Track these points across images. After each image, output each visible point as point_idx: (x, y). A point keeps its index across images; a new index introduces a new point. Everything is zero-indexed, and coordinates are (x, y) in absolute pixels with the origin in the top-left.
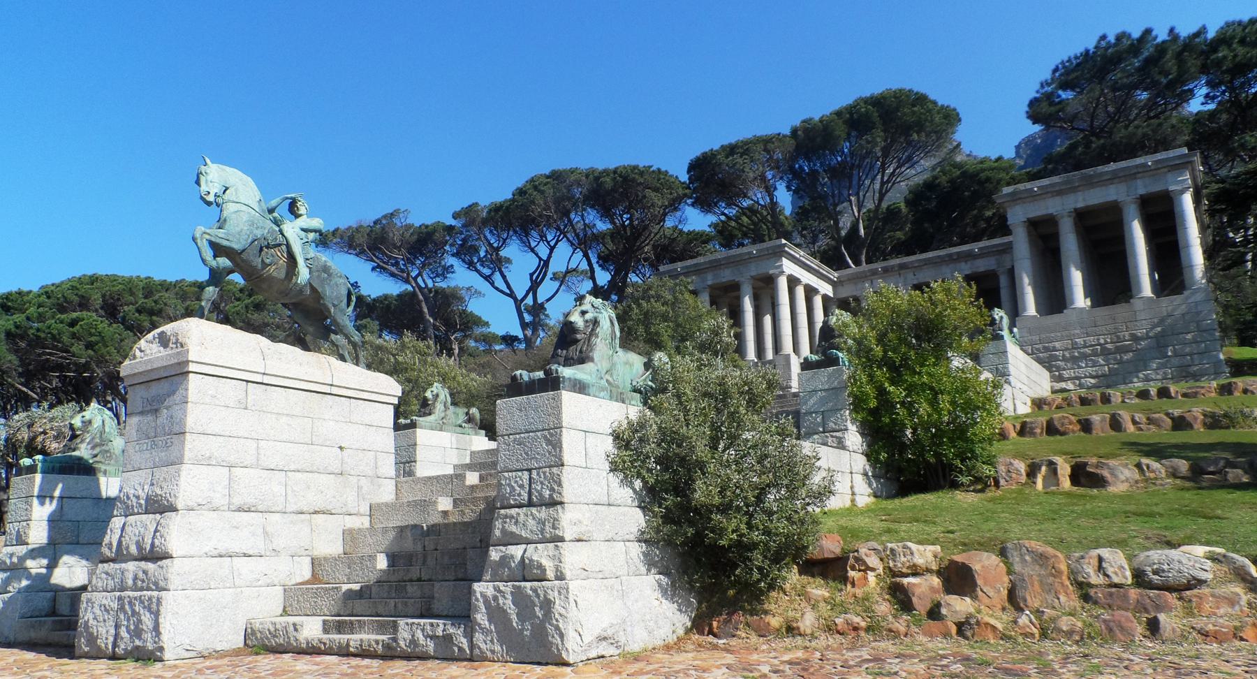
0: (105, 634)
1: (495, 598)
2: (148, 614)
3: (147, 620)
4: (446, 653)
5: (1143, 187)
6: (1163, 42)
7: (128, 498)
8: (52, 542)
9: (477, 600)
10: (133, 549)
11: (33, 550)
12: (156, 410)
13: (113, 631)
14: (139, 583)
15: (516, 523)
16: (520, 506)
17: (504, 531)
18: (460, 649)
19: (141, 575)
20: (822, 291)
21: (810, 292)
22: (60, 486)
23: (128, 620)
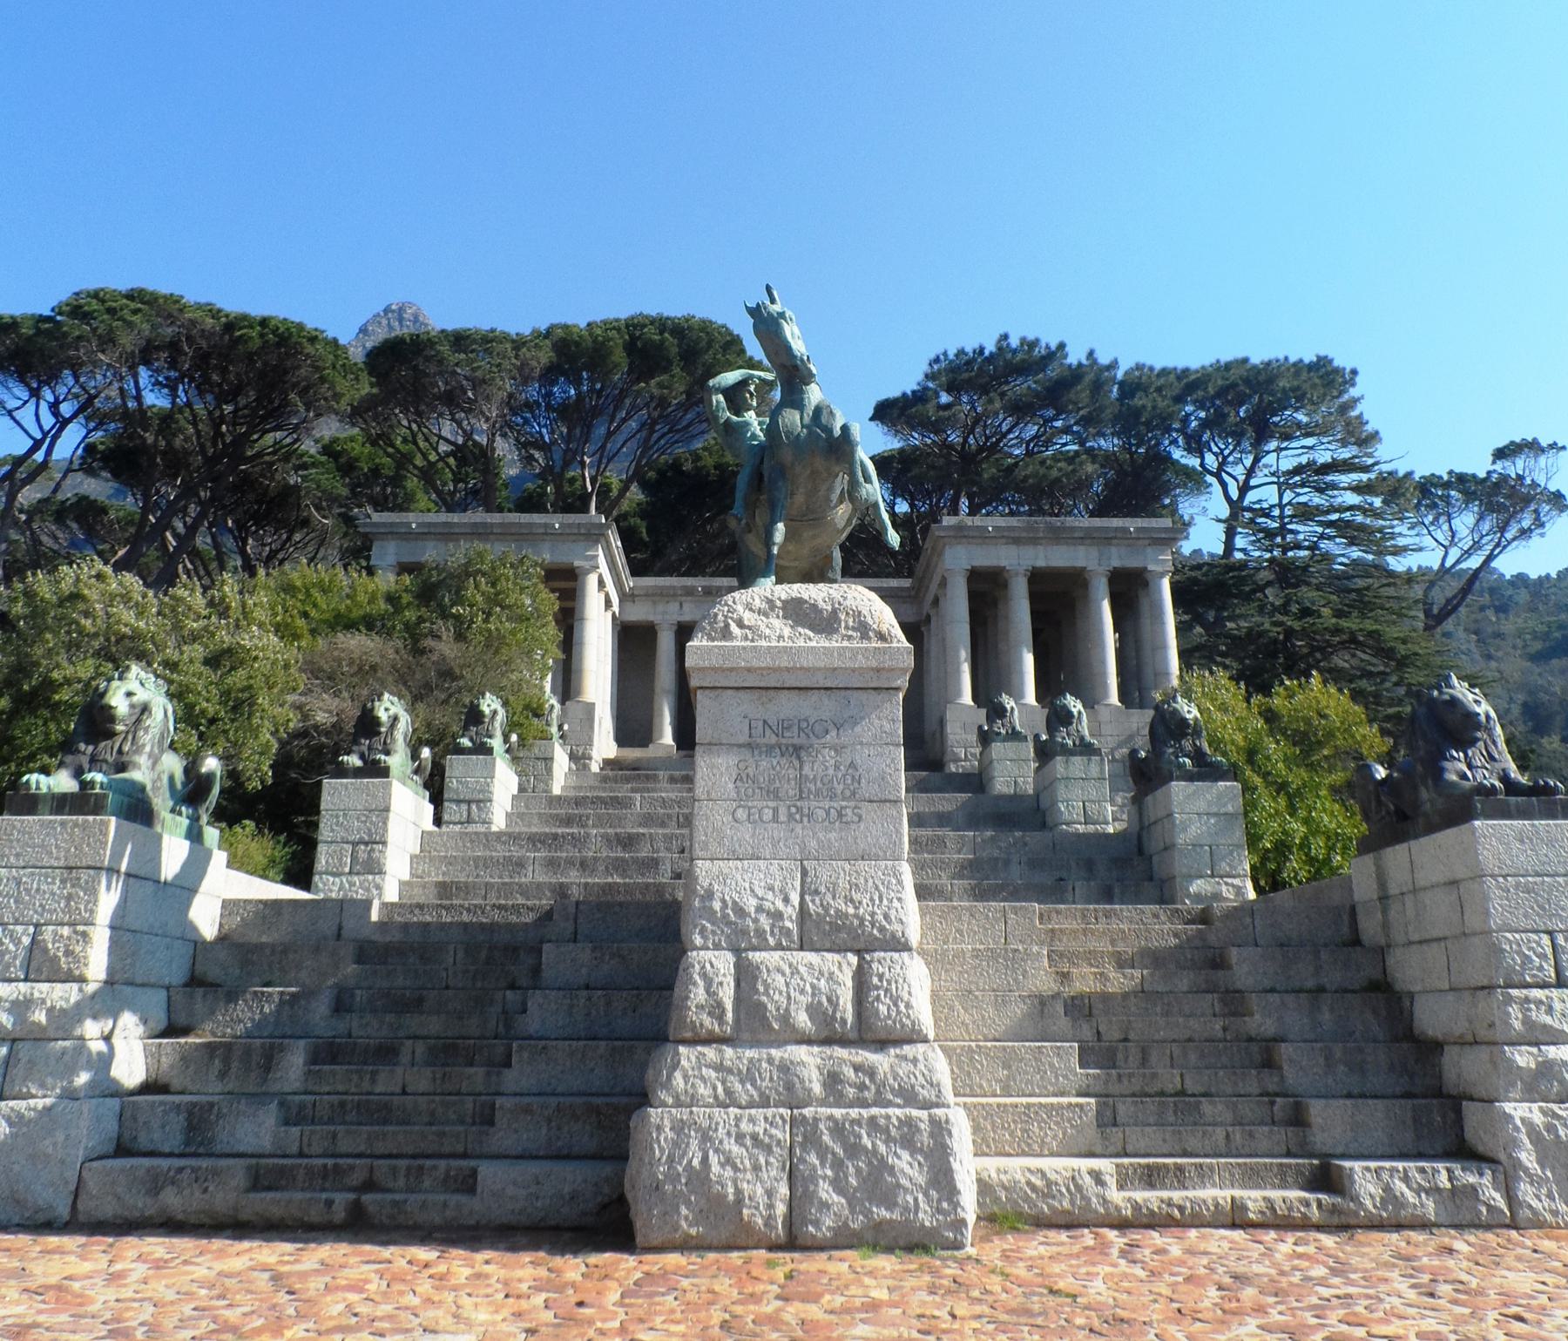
0: (764, 1195)
1: (1550, 1128)
2: (905, 1155)
3: (908, 1168)
4: (1462, 1213)
5: (1119, 558)
6: (1080, 365)
7: (740, 911)
8: (109, 983)
9: (1517, 1129)
10: (802, 1020)
11: (94, 996)
12: (797, 750)
13: (784, 1190)
14: (851, 1092)
15: (1550, 1011)
16: (1544, 985)
17: (1527, 1021)
18: (1490, 1208)
19: (849, 1073)
22: (129, 847)
23: (838, 1165)
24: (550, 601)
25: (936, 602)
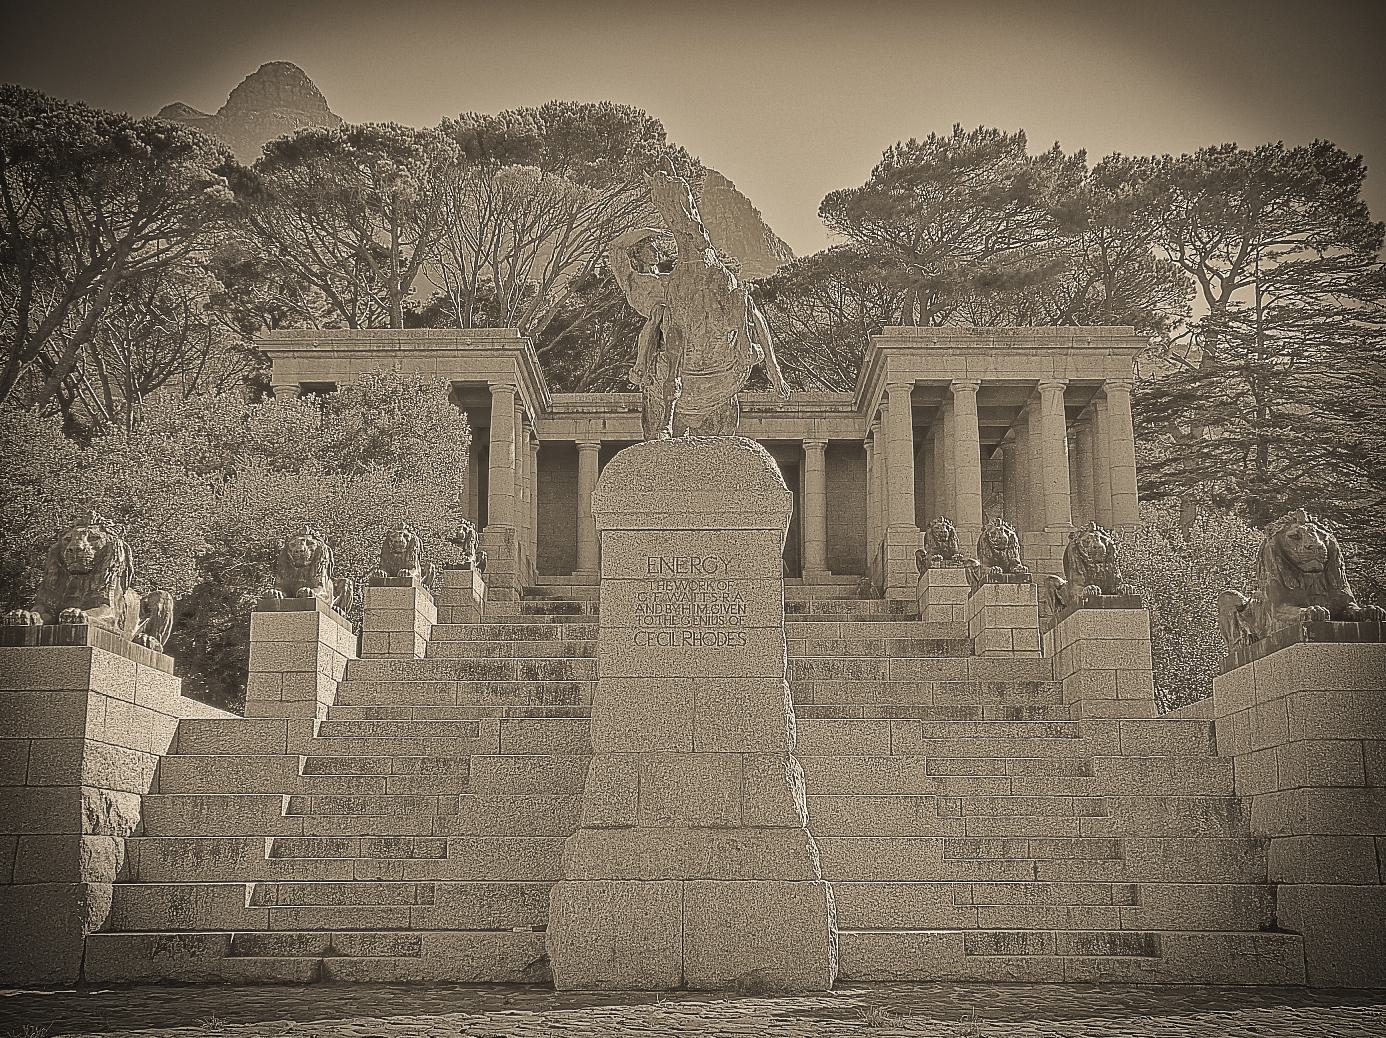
24: (458, 417)
25: (878, 417)
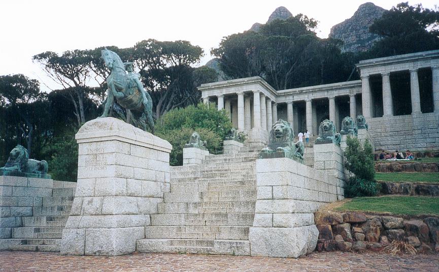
5: (421, 65)
20: (272, 100)
21: (267, 99)
